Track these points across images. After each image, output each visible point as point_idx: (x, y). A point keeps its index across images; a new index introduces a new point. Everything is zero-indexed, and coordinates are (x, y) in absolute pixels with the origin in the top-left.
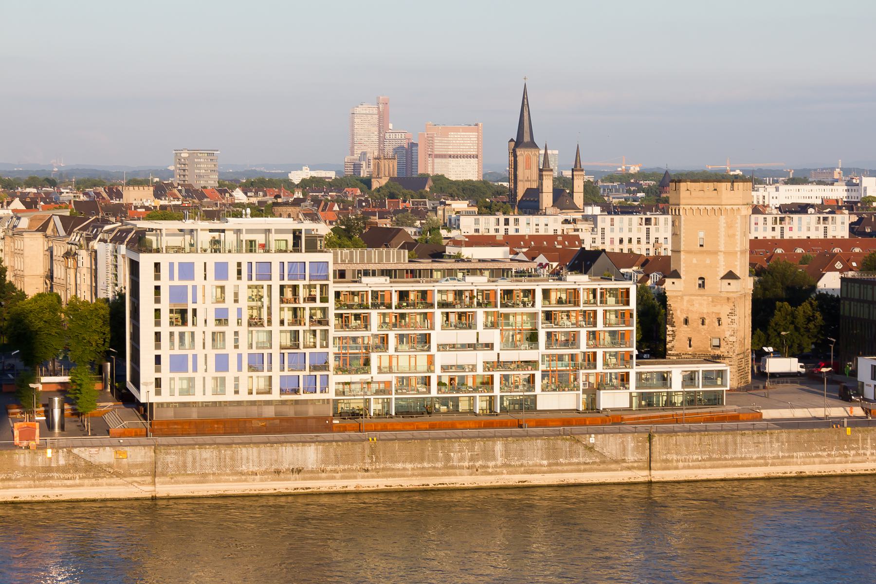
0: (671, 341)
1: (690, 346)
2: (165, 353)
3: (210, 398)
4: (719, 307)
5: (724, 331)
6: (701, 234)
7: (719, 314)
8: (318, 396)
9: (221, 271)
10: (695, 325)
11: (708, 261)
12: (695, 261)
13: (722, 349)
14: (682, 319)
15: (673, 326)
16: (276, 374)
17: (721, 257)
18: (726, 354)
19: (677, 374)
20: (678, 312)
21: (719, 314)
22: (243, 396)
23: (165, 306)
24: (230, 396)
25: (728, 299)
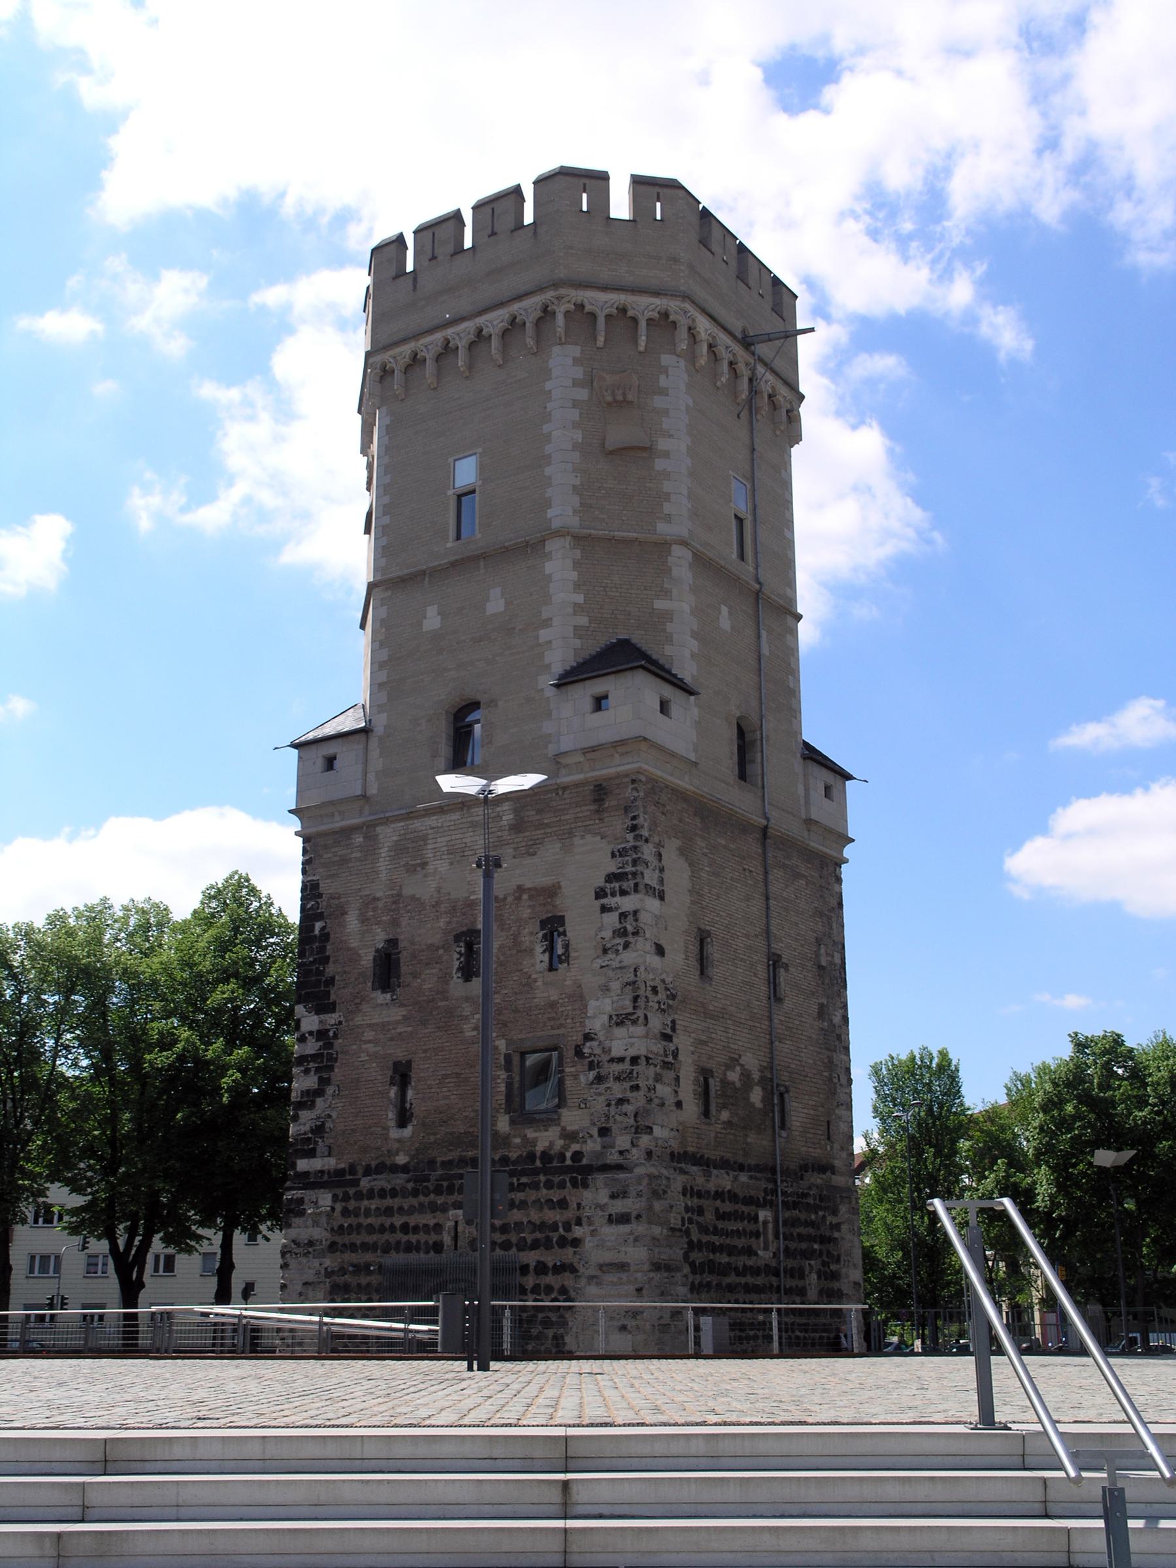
0: (310, 1098)
1: (403, 1119)
4: (551, 850)
5: (579, 998)
6: (466, 472)
7: (551, 892)
10: (428, 981)
11: (495, 605)
12: (432, 621)
13: (572, 1118)
14: (367, 959)
15: (323, 1006)
17: (559, 565)
18: (592, 1146)
20: (352, 921)
21: (551, 892)
25: (600, 792)
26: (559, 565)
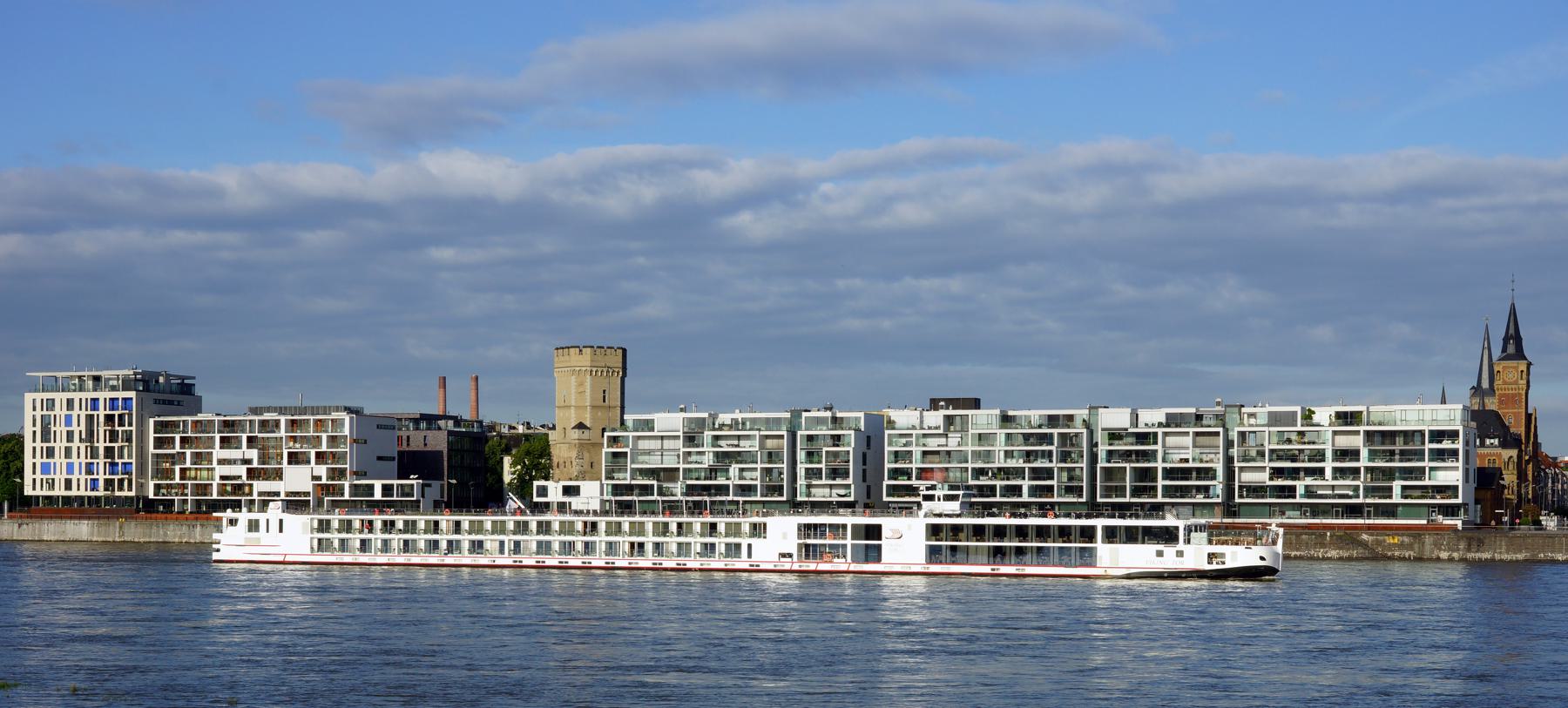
2: (38, 461)
3: (64, 493)
8: (126, 493)
9: (70, 403)
16: (101, 478)
17: (573, 410)
19: (378, 485)
22: (82, 493)
23: (38, 429)
24: (74, 492)
26: (573, 410)
